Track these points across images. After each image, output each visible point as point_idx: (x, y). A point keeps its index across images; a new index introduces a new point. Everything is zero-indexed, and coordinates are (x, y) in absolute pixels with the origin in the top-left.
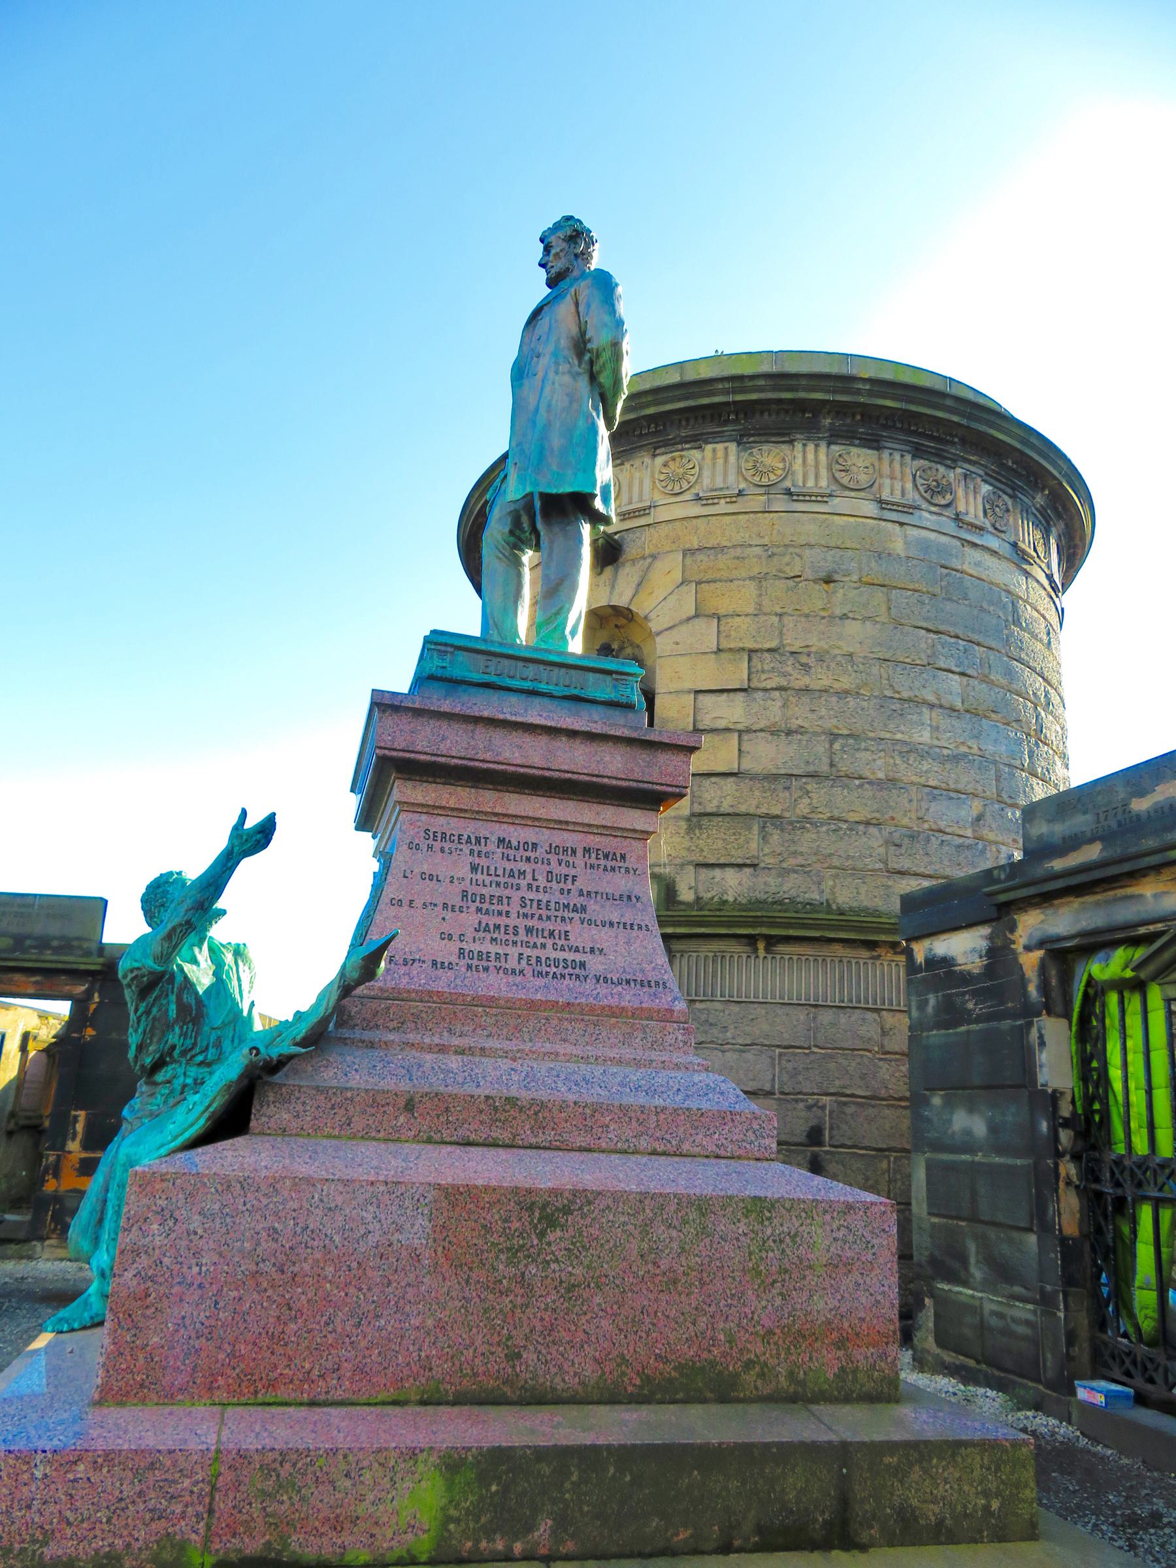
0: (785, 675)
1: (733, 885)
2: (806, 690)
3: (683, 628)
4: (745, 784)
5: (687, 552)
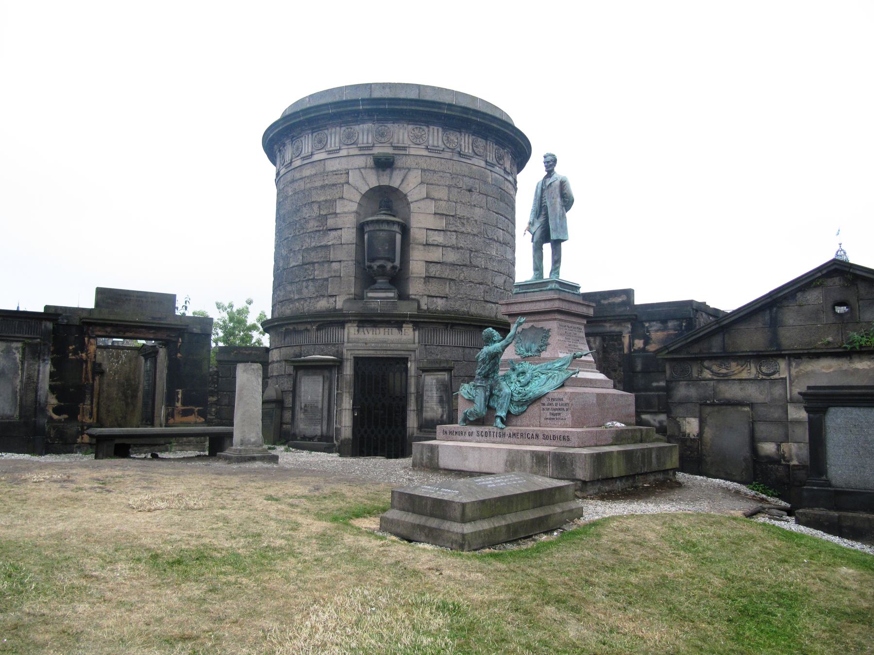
0: (457, 226)
1: (440, 304)
2: (462, 233)
3: (422, 202)
4: (444, 267)
5: (423, 170)
